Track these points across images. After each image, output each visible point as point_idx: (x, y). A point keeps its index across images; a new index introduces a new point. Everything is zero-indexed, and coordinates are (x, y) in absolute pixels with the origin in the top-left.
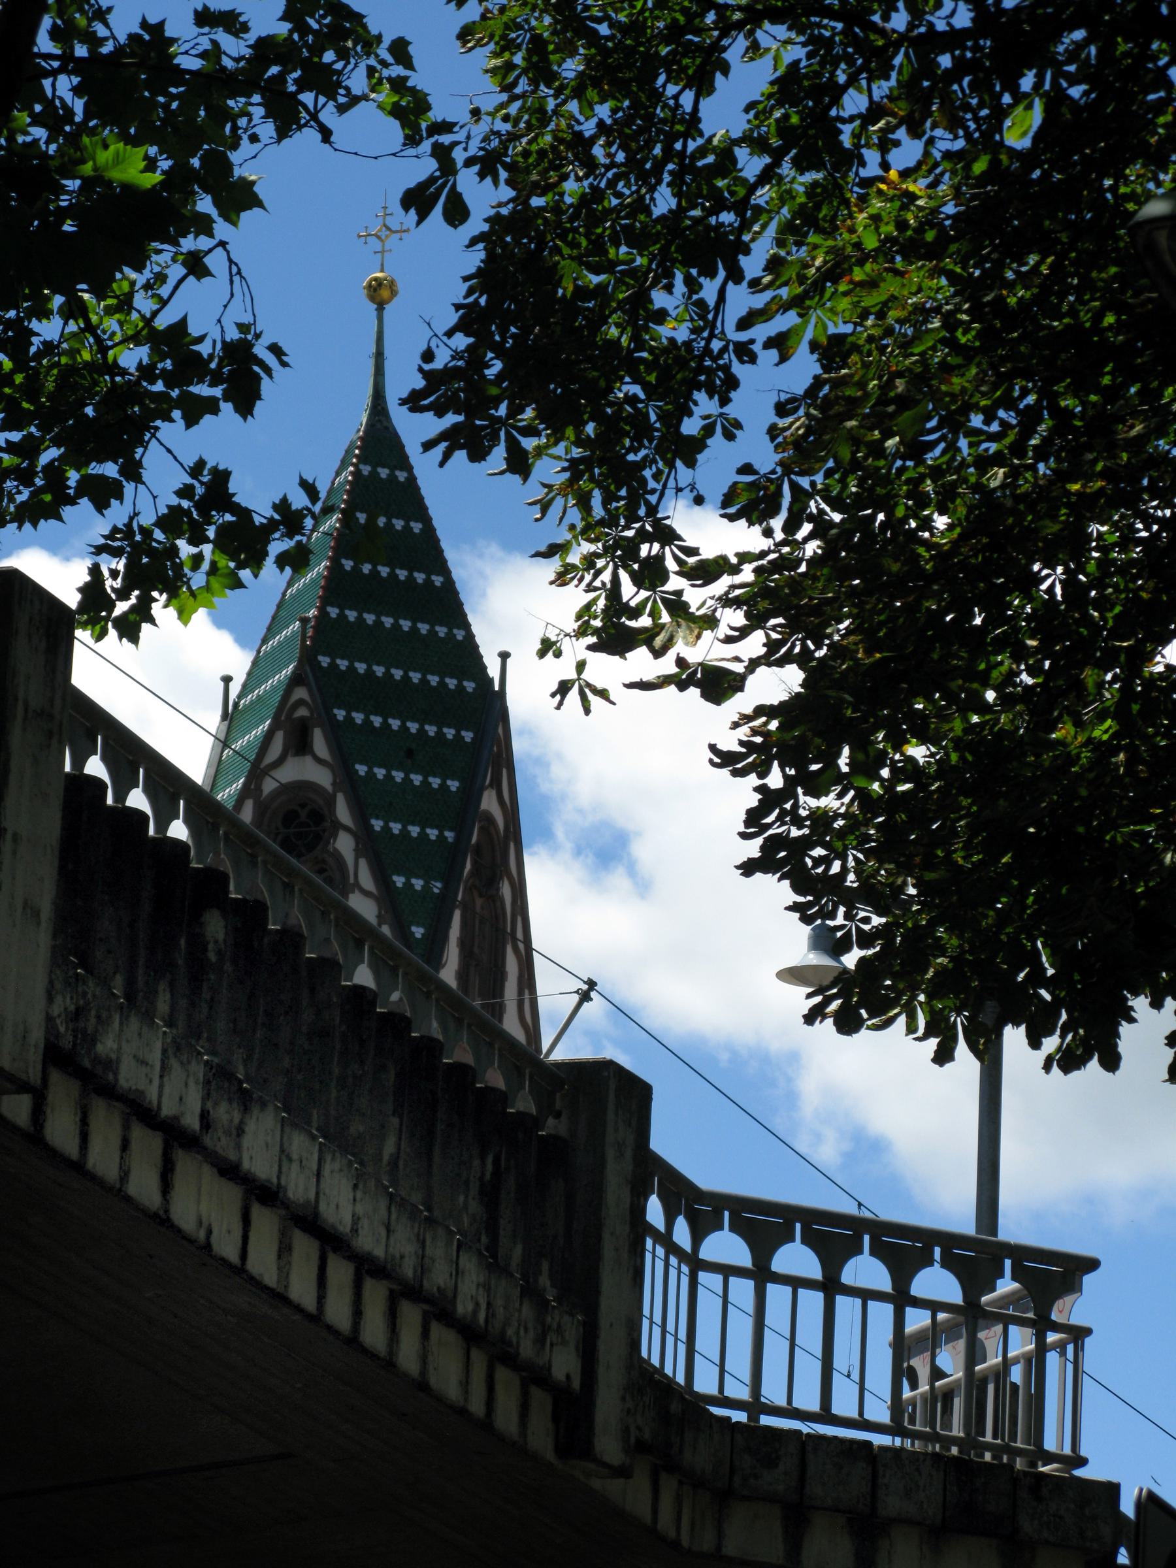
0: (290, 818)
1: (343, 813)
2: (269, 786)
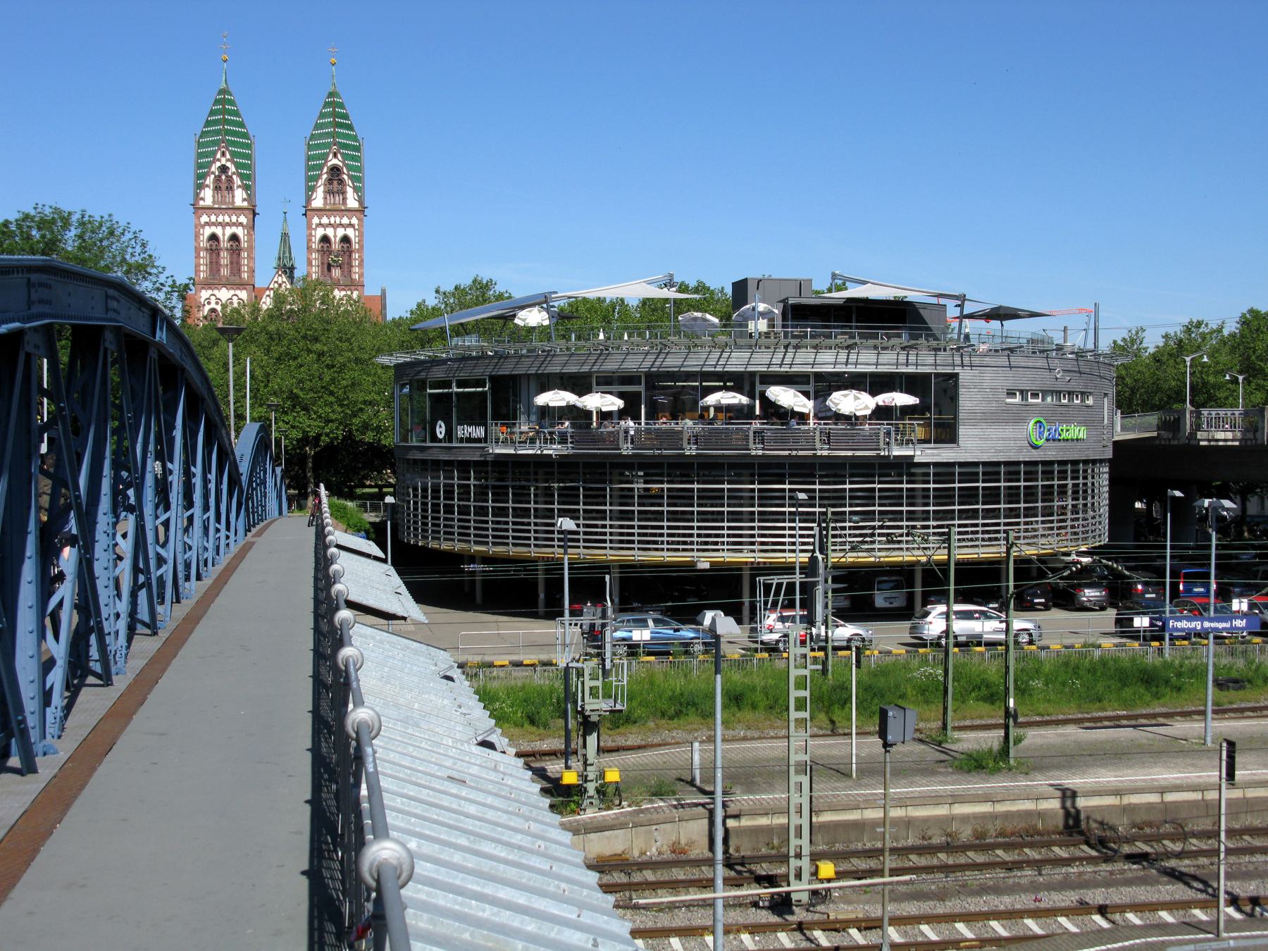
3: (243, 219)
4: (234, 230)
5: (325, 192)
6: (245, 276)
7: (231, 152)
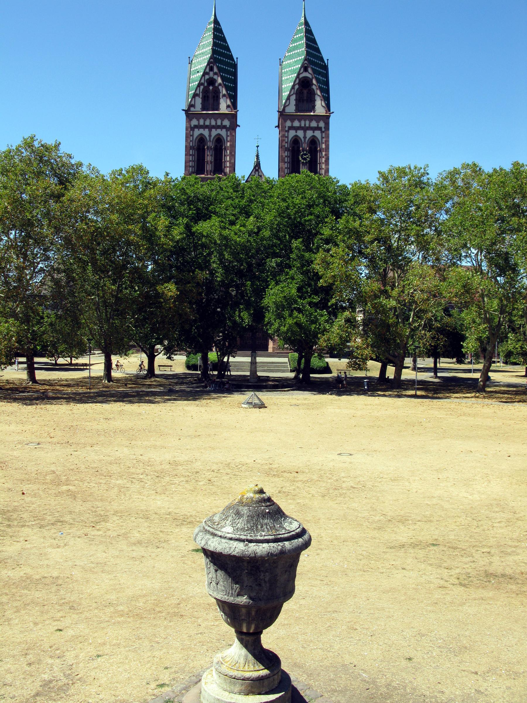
0: (303, 82)
1: (314, 82)
2: (301, 76)
3: (226, 123)
4: (219, 131)
5: (296, 100)
6: (227, 170)
7: (218, 67)
